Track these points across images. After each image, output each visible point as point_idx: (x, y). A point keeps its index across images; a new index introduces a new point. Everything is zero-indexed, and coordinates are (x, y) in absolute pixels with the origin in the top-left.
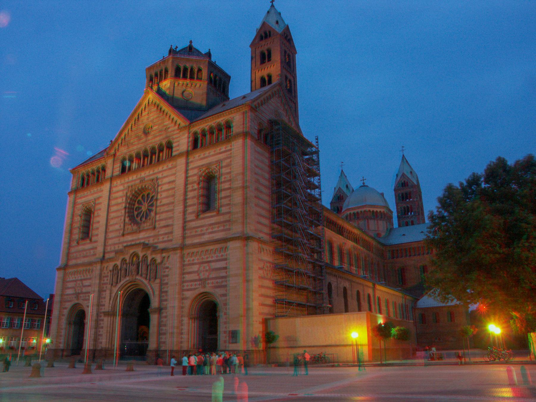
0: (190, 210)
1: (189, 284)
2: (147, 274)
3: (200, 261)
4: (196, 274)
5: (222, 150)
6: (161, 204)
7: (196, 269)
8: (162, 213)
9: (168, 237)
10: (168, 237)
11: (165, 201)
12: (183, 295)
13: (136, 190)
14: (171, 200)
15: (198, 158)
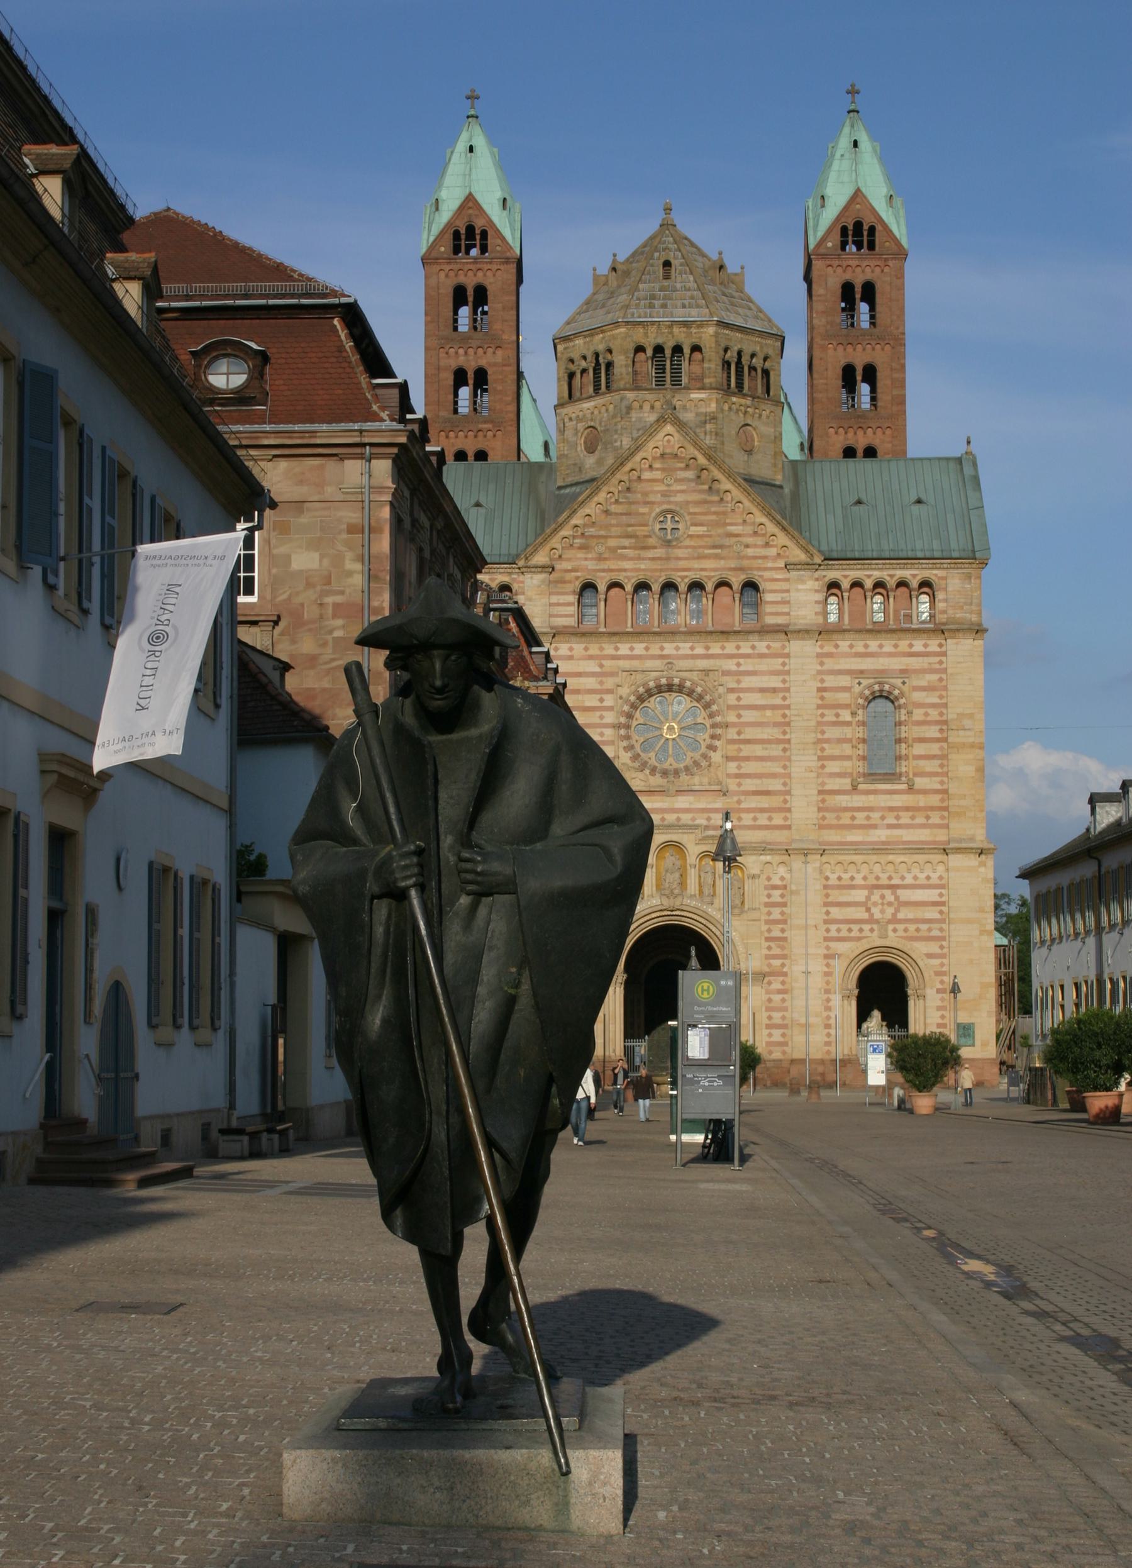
0: (833, 767)
1: (844, 927)
2: (714, 895)
3: (872, 881)
4: (864, 909)
5: (914, 649)
6: (742, 737)
7: (864, 900)
8: (747, 759)
9: (770, 819)
10: (770, 819)
11: (749, 733)
12: (828, 948)
13: (652, 684)
14: (775, 733)
15: (847, 650)
